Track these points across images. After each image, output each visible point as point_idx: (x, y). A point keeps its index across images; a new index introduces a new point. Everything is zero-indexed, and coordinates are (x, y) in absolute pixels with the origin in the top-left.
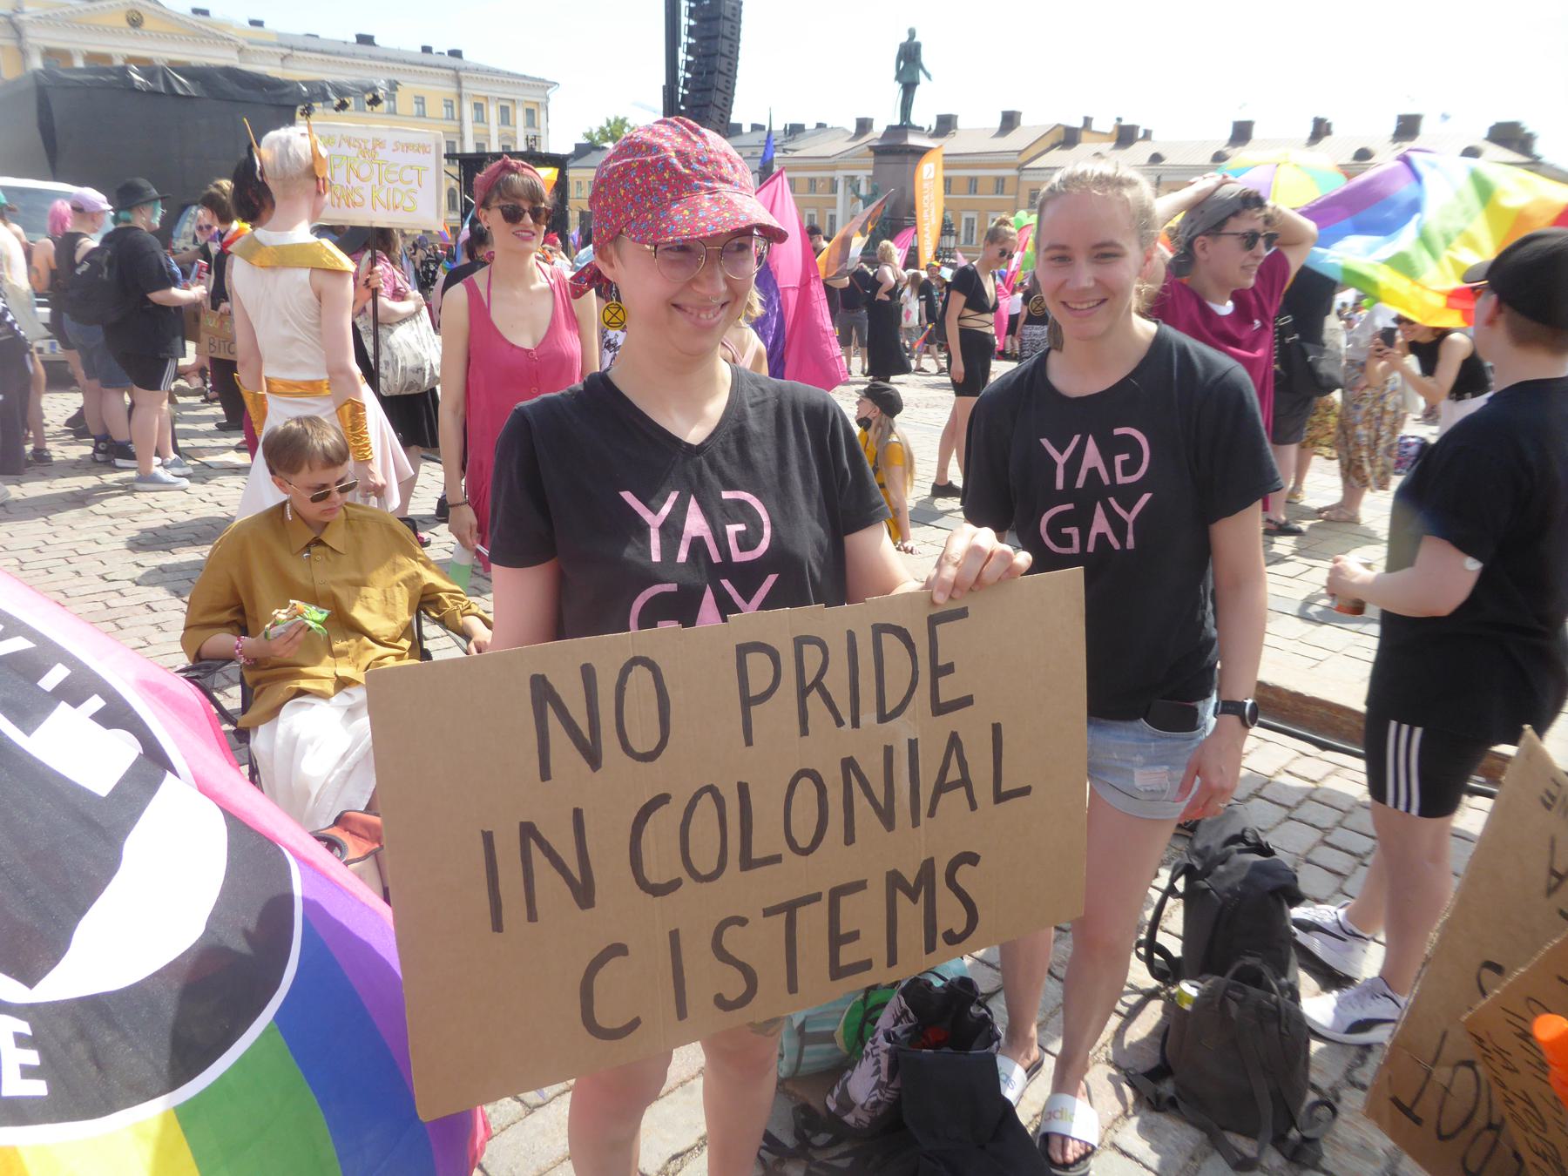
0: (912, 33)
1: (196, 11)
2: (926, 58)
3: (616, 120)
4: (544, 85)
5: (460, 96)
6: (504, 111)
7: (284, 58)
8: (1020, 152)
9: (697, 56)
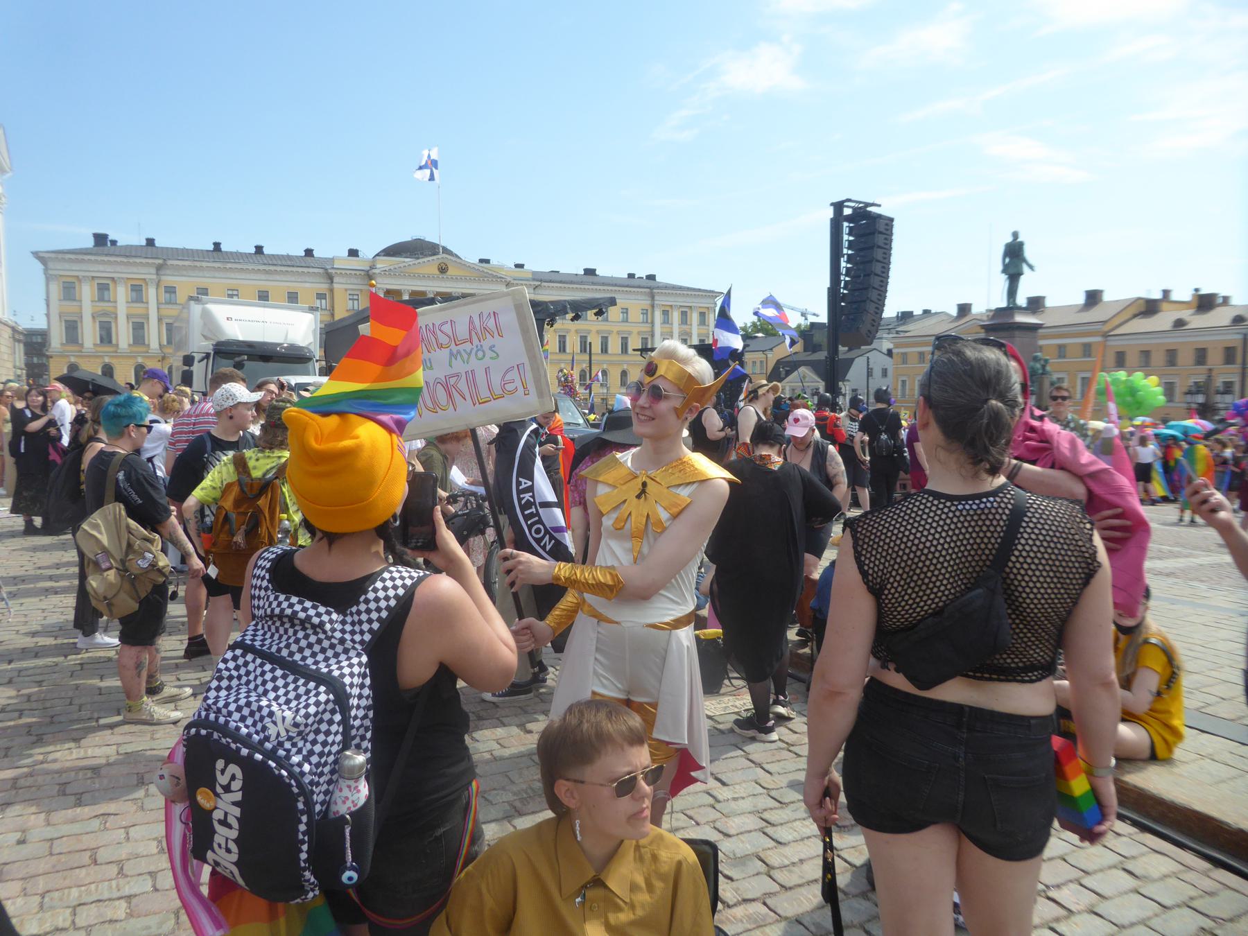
0: (1015, 235)
1: (481, 261)
2: (1028, 253)
5: (653, 306)
6: (684, 314)
7: (536, 288)
8: (1105, 322)
9: (855, 264)
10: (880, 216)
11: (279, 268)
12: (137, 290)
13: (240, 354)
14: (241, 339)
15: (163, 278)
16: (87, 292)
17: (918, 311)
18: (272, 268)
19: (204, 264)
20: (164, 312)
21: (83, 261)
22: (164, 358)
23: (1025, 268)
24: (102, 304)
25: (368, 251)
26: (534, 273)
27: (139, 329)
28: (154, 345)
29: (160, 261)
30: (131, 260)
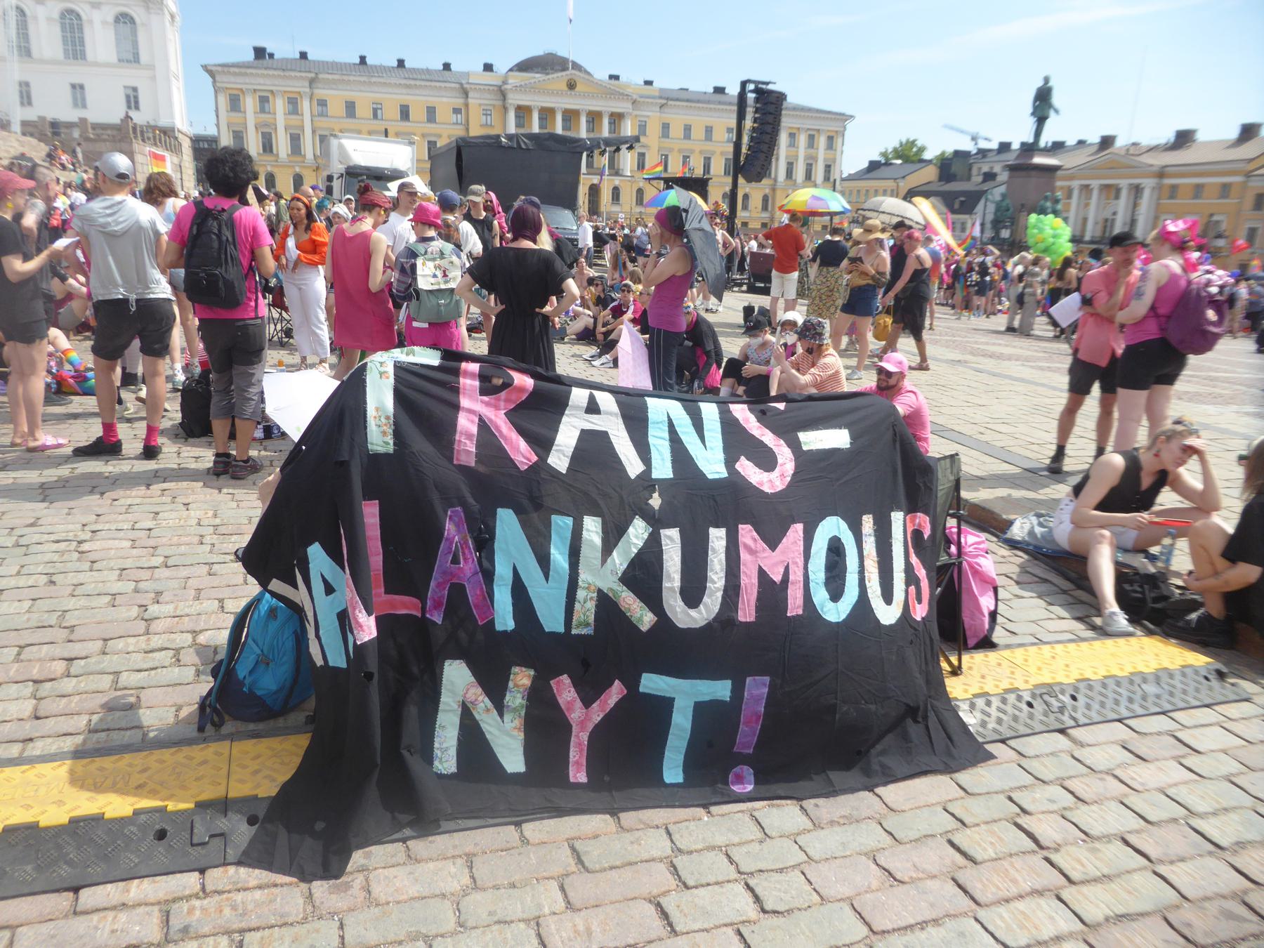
0: (1047, 80)
1: (611, 77)
2: (1056, 99)
3: (908, 141)
4: (843, 118)
6: (811, 138)
7: (662, 106)
8: (1251, 160)
10: (772, 92)
11: (418, 83)
12: (293, 103)
13: (362, 175)
14: (363, 164)
15: (316, 91)
16: (250, 104)
17: (1071, 142)
18: (412, 82)
19: (352, 78)
20: (317, 124)
21: (246, 74)
22: (318, 168)
23: (1052, 113)
24: (263, 115)
25: (503, 65)
26: (661, 90)
27: (295, 140)
28: (309, 155)
29: (313, 75)
30: (287, 74)
